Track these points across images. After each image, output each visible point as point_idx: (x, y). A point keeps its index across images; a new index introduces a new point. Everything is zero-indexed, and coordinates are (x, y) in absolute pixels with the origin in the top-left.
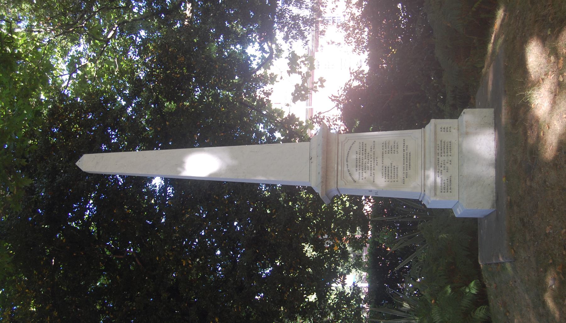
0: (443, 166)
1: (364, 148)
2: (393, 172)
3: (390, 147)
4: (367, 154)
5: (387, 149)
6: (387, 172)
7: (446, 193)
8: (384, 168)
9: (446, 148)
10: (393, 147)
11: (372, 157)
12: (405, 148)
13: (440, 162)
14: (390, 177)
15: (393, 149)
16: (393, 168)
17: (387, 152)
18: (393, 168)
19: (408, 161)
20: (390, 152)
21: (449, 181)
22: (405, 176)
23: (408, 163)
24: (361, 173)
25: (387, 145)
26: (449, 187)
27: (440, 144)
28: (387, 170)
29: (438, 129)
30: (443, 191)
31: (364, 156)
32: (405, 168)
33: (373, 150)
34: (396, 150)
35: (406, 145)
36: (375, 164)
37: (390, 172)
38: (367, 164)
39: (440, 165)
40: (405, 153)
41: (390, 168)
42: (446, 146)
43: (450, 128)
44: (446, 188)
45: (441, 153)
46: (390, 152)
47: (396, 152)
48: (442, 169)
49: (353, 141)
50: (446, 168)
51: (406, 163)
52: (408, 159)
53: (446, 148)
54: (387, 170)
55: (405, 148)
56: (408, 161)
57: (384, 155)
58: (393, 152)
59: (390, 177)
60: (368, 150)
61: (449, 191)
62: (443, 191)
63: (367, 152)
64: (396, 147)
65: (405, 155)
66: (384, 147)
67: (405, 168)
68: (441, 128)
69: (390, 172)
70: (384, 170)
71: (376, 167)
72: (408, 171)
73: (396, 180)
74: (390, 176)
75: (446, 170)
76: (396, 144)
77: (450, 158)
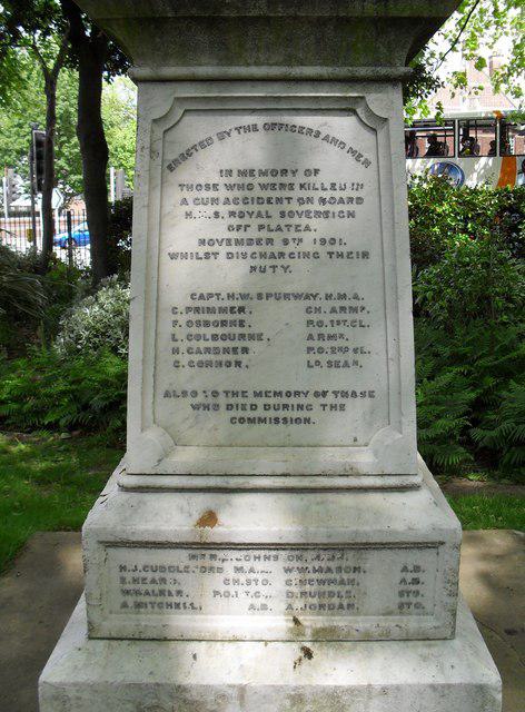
0: (243, 578)
1: (337, 208)
3: (336, 330)
5: (326, 318)
8: (237, 303)
11: (291, 247)
12: (330, 399)
14: (194, 330)
15: (327, 344)
16: (239, 344)
17: (315, 317)
18: (239, 344)
19: (271, 414)
20: (315, 331)
22: (200, 399)
23: (260, 413)
24: (211, 194)
25: (348, 317)
27: (344, 564)
28: (228, 317)
32: (240, 400)
34: (324, 358)
35: (349, 402)
40: (310, 399)
41: (237, 330)
44: (143, 588)
46: (315, 331)
47: (313, 357)
49: (370, 156)
51: (261, 402)
52: (281, 414)
54: (228, 317)
55: (330, 399)
56: (271, 414)
58: (316, 344)
59: (194, 330)
61: (131, 600)
62: (129, 576)
64: (339, 357)
65: (302, 400)
66: (338, 304)
67: (240, 400)
68: (417, 569)
70: (228, 303)
72: (226, 415)
73: (184, 359)
74: (203, 330)
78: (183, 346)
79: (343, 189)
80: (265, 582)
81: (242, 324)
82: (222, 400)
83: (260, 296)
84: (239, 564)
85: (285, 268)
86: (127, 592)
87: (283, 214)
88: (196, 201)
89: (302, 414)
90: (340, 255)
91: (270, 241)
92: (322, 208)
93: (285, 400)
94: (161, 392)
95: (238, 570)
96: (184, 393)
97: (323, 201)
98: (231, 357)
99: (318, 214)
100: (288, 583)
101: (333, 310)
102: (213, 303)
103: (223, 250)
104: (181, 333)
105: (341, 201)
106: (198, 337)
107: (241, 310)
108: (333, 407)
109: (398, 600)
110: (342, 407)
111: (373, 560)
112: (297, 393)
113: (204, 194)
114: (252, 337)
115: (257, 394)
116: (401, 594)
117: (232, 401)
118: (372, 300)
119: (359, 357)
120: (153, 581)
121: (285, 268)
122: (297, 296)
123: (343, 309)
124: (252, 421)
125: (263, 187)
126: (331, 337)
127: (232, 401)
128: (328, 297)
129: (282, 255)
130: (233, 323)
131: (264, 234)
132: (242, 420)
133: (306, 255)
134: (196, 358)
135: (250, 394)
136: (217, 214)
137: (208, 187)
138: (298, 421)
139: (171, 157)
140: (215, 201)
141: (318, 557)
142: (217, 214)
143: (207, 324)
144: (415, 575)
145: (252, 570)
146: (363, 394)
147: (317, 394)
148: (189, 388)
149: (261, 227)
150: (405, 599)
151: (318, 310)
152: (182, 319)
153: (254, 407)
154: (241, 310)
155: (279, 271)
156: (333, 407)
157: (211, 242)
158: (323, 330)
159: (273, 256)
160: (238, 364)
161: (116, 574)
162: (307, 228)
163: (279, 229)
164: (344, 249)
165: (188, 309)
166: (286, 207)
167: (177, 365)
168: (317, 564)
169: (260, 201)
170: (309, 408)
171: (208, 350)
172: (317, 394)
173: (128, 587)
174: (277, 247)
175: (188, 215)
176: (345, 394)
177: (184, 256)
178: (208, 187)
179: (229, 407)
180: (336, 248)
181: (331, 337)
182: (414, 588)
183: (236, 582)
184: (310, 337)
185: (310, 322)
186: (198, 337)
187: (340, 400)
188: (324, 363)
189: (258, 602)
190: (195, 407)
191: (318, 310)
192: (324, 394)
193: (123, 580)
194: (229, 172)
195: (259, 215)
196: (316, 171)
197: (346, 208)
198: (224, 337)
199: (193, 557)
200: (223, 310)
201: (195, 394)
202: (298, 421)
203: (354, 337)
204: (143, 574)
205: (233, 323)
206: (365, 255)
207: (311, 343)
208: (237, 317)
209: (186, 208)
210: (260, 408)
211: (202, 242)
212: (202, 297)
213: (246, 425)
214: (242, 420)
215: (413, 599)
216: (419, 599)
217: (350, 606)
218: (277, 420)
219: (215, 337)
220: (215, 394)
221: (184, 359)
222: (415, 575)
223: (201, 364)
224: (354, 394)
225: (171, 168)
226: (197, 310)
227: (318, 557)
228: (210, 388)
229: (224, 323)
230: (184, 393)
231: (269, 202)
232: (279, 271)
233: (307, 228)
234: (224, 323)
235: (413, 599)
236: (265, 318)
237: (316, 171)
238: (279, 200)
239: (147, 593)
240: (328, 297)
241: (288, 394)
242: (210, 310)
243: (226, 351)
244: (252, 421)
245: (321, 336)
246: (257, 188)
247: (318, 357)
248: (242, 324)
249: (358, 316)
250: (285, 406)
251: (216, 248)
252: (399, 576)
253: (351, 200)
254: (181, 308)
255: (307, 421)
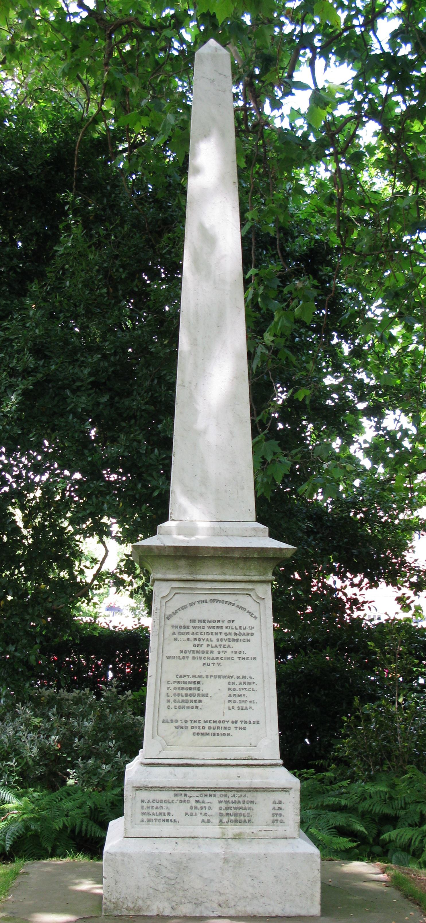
0: (199, 806)
2: (189, 698)
3: (242, 692)
4: (227, 643)
5: (237, 687)
6: (189, 686)
7: (138, 810)
9: (238, 811)
10: (242, 699)
11: (222, 655)
13: (207, 799)
14: (177, 692)
15: (237, 699)
17: (232, 686)
19: (212, 731)
20: (232, 693)
21: (167, 817)
22: (179, 724)
23: (206, 730)
24: (186, 630)
26: (154, 817)
27: (246, 799)
28: (193, 686)
29: (278, 796)
30: (145, 805)
31: (223, 636)
32: (197, 724)
33: (236, 656)
34: (236, 705)
36: (207, 661)
37: (189, 692)
38: (205, 643)
39: (201, 799)
41: (197, 692)
42: (241, 811)
43: (282, 821)
44: (151, 811)
45: (227, 802)
46: (232, 693)
47: (231, 705)
48: (193, 804)
49: (256, 614)
50: (194, 811)
51: (207, 725)
52: (216, 731)
53: (238, 811)
54: (193, 686)
55: (239, 725)
56: (212, 731)
57: (227, 680)
59: (177, 692)
60: (237, 646)
61: (145, 818)
62: (145, 805)
63: (232, 644)
64: (243, 705)
65: (226, 725)
67: (197, 724)
68: (280, 802)
69: (189, 692)
71: (200, 663)
74: (181, 692)
75: (189, 811)
76: (248, 705)
77: (216, 820)
78: (172, 699)
79: (245, 629)
80: (210, 808)
81: (199, 689)
82: (189, 725)
83: (207, 677)
84: (197, 799)
85: (219, 664)
86: (144, 814)
87: (218, 640)
88: (179, 633)
89: (226, 732)
90: (243, 659)
91: (212, 652)
92: (235, 638)
93: (218, 725)
94: (161, 720)
95: (197, 802)
96: (172, 721)
97: (236, 634)
98: (193, 704)
99: (234, 640)
100: (220, 808)
101: (240, 684)
102: (186, 679)
103: (191, 655)
104: (171, 693)
105: (244, 634)
106: (179, 695)
107: (199, 683)
108: (240, 728)
109: (272, 818)
110: (244, 728)
111: (260, 797)
112: (224, 722)
113: (183, 630)
114: (203, 695)
115: (206, 722)
116: (273, 815)
117: (194, 725)
118: (257, 678)
119: (252, 705)
120: (157, 808)
121: (219, 664)
122: (224, 677)
123: (245, 683)
124: (202, 734)
125: (209, 628)
126: (239, 696)
127: (194, 725)
128: (238, 677)
129: (217, 658)
130: (195, 689)
131: (209, 649)
132: (198, 734)
133: (228, 658)
134: (178, 704)
135: (202, 722)
136: (188, 639)
137: (184, 627)
138: (224, 734)
139: (168, 613)
140: (188, 633)
141: (234, 796)
142: (188, 639)
143: (183, 689)
144: (279, 805)
145: (203, 802)
146: (254, 722)
147: (233, 722)
148: (174, 718)
149: (208, 646)
150: (275, 818)
151: (233, 683)
152: (172, 686)
153: (204, 728)
154: (199, 683)
155: (216, 665)
156: (240, 728)
157: (186, 652)
158: (235, 692)
159: (213, 659)
160: (197, 707)
161: (139, 804)
162: (229, 646)
163: (216, 646)
164: (245, 656)
165: (175, 682)
166: (219, 637)
167: (168, 707)
168: (233, 799)
169: (208, 634)
170: (229, 728)
171: (183, 701)
172: (233, 722)
173: (144, 811)
174: (215, 655)
175: (176, 639)
176: (246, 722)
177: (173, 658)
178: (184, 627)
179: (192, 728)
180: (242, 655)
181: (239, 696)
182: (279, 812)
183: (196, 808)
184: (230, 696)
185: (230, 689)
186: (179, 695)
187: (243, 725)
188: (236, 708)
189: (206, 818)
190: (177, 728)
191: (233, 683)
192: (236, 722)
193: (142, 808)
194: (194, 621)
195: (207, 640)
196: (233, 621)
197: (246, 637)
198: (191, 695)
199: (176, 795)
200: (190, 683)
201: (177, 721)
202: (224, 734)
203: (251, 696)
204: (153, 804)
205: (195, 689)
206: (255, 659)
207: (230, 699)
208: (197, 686)
209: (175, 636)
210: (207, 728)
211: (181, 652)
212: (181, 676)
213: (200, 736)
214: (198, 734)
215: (279, 818)
216: (282, 818)
217: (249, 821)
218: (214, 734)
219: (186, 695)
220: (186, 721)
221: (172, 705)
222: (279, 805)
223: (180, 707)
224: (250, 722)
225: (168, 618)
226: (179, 682)
227: (234, 796)
228: (184, 718)
229: (191, 689)
230: (172, 721)
231: (212, 634)
232: (216, 665)
233: (229, 646)
234: (191, 689)
235: (279, 818)
236: (209, 686)
237: (233, 621)
238: (216, 634)
239: (154, 814)
240: (238, 677)
241: (220, 722)
242: (185, 683)
243: (191, 701)
244: (202, 734)
245: (235, 695)
246: (206, 628)
247: (233, 705)
248: (199, 689)
249: (252, 686)
250: (218, 728)
251: (187, 654)
252: (272, 806)
253: (248, 634)
254: (171, 681)
255: (228, 734)
